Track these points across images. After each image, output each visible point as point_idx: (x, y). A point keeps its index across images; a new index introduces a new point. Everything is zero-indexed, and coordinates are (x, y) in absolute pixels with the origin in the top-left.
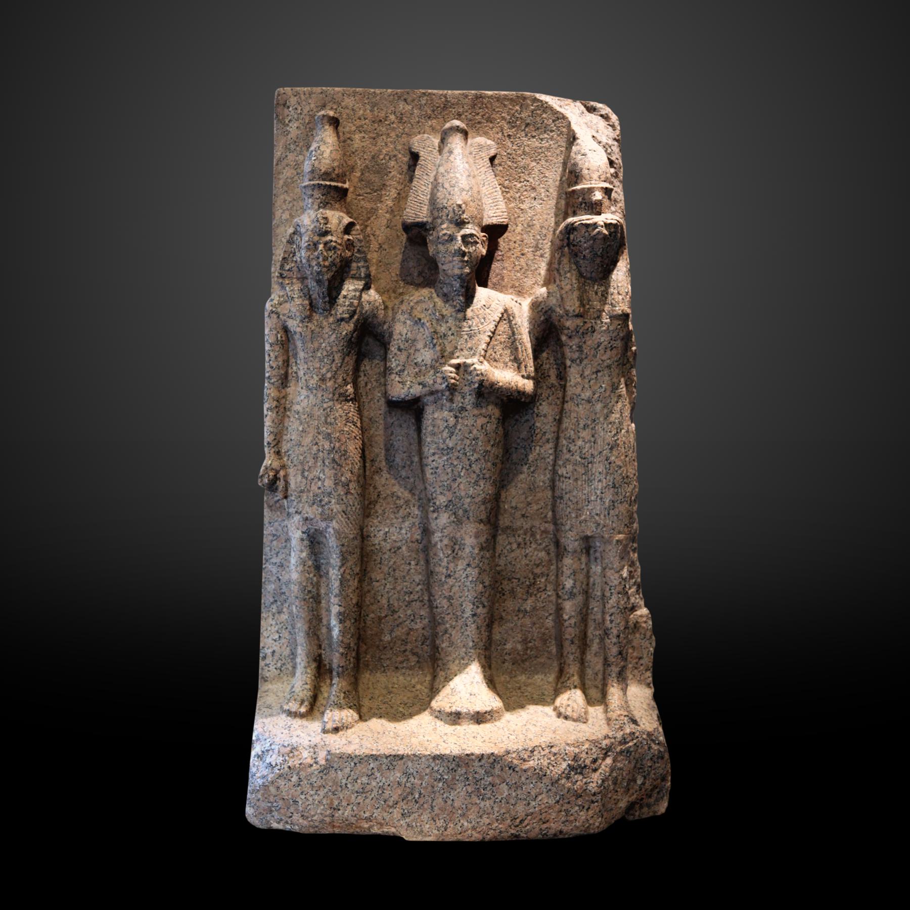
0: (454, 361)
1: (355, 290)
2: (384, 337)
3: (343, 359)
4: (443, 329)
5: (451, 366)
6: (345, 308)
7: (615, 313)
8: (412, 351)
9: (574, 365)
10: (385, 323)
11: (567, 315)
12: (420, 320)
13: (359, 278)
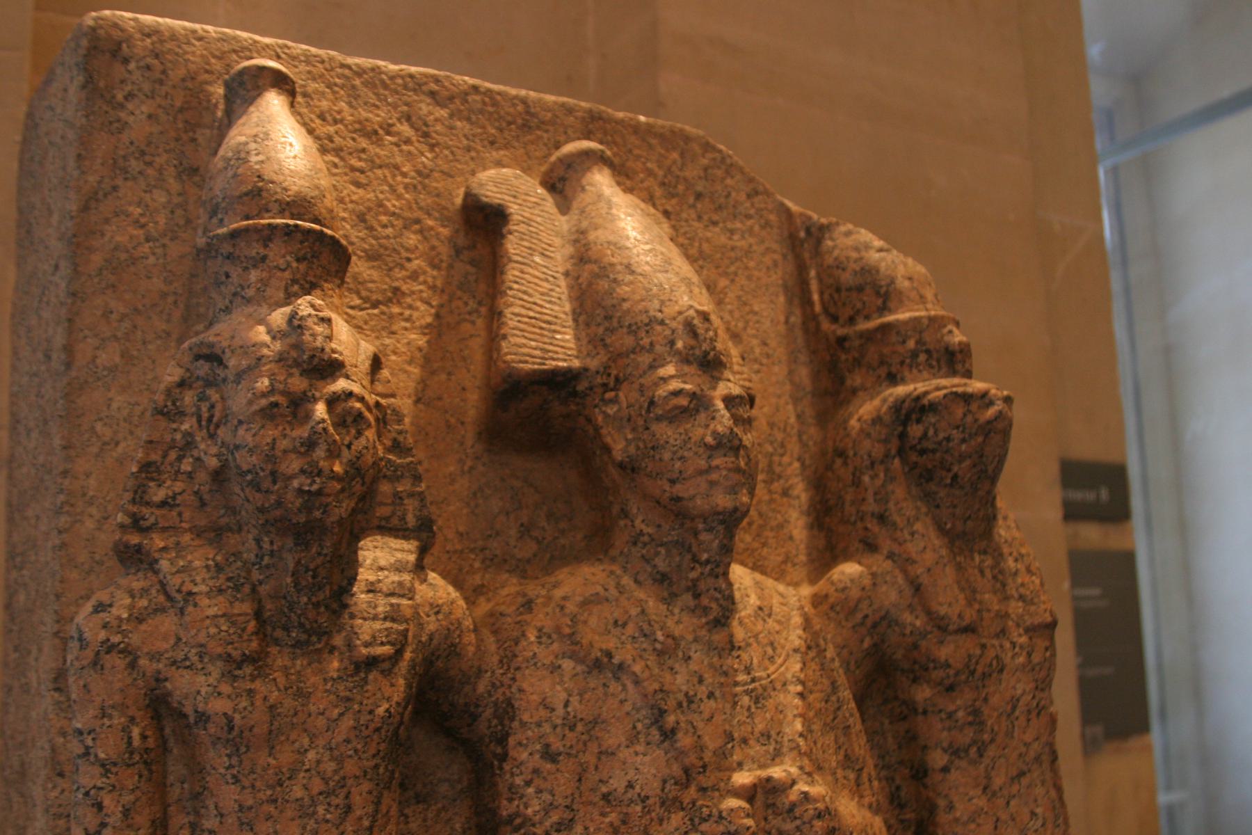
0: (742, 778)
1: (398, 568)
2: (475, 717)
3: (378, 803)
4: (680, 679)
5: (736, 793)
6: (377, 625)
7: (1037, 620)
8: (589, 758)
9: (963, 764)
10: (480, 672)
11: (943, 629)
12: (609, 655)
13: (399, 532)
